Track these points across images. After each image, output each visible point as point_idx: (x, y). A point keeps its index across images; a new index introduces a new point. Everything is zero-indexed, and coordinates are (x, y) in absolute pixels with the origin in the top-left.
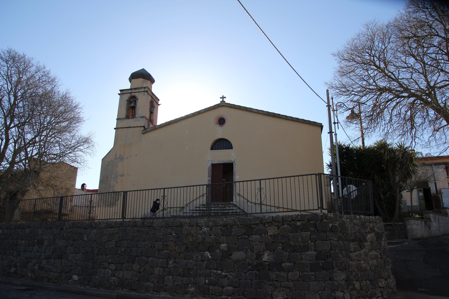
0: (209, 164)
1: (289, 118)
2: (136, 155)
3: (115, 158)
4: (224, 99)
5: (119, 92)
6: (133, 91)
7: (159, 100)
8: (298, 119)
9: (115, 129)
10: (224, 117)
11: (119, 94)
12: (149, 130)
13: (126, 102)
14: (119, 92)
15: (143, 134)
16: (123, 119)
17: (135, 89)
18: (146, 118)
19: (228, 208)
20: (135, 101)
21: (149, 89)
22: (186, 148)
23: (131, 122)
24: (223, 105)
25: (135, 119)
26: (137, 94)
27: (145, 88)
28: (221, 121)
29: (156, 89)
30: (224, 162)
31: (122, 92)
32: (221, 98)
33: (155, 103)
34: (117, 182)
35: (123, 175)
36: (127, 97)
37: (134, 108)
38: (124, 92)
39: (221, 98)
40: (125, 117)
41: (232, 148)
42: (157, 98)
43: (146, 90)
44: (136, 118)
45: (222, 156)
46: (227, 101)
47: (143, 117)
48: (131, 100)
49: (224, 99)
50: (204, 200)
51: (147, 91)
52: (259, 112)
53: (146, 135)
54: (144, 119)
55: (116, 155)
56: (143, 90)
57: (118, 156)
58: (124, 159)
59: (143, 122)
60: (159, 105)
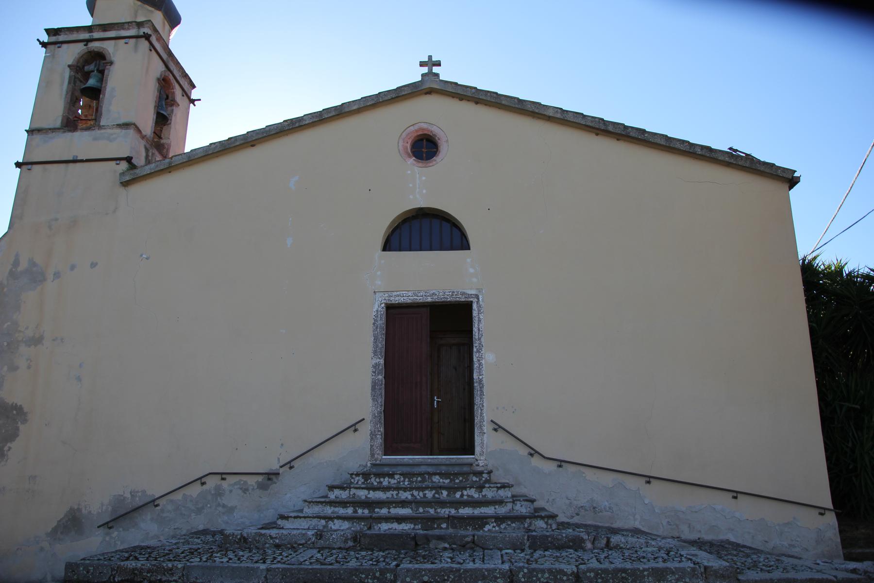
0: (377, 307)
1: (678, 146)
2: (94, 265)
3: (12, 274)
4: (435, 70)
5: (45, 38)
6: (96, 35)
7: (194, 87)
8: (709, 149)
9: (18, 165)
10: (435, 130)
11: (44, 45)
12: (147, 170)
13: (67, 73)
14: (45, 38)
15: (126, 184)
16: (53, 130)
17: (105, 27)
18: (139, 131)
19: (473, 493)
20: (102, 72)
21: (155, 30)
22: (289, 242)
23: (80, 143)
24: (430, 87)
25: (97, 132)
26: (109, 47)
27: (140, 25)
28: (425, 147)
29: (179, 42)
30: (435, 299)
31: (54, 39)
32: (422, 64)
33: (178, 92)
34: (14, 368)
35: (37, 341)
36: (71, 53)
37: (95, 93)
38: (61, 38)
39: (422, 64)
40: (58, 124)
41: (469, 249)
42: (186, 76)
43: (147, 30)
44: (100, 127)
45: (427, 276)
46: (445, 74)
47: (126, 126)
48: (87, 68)
49: (435, 70)
50: (361, 447)
51: (147, 37)
52: (570, 118)
53: (136, 189)
54: (131, 131)
55: (16, 263)
56: (132, 32)
57: (24, 265)
58: (45, 280)
59: (125, 144)
60: (193, 101)
